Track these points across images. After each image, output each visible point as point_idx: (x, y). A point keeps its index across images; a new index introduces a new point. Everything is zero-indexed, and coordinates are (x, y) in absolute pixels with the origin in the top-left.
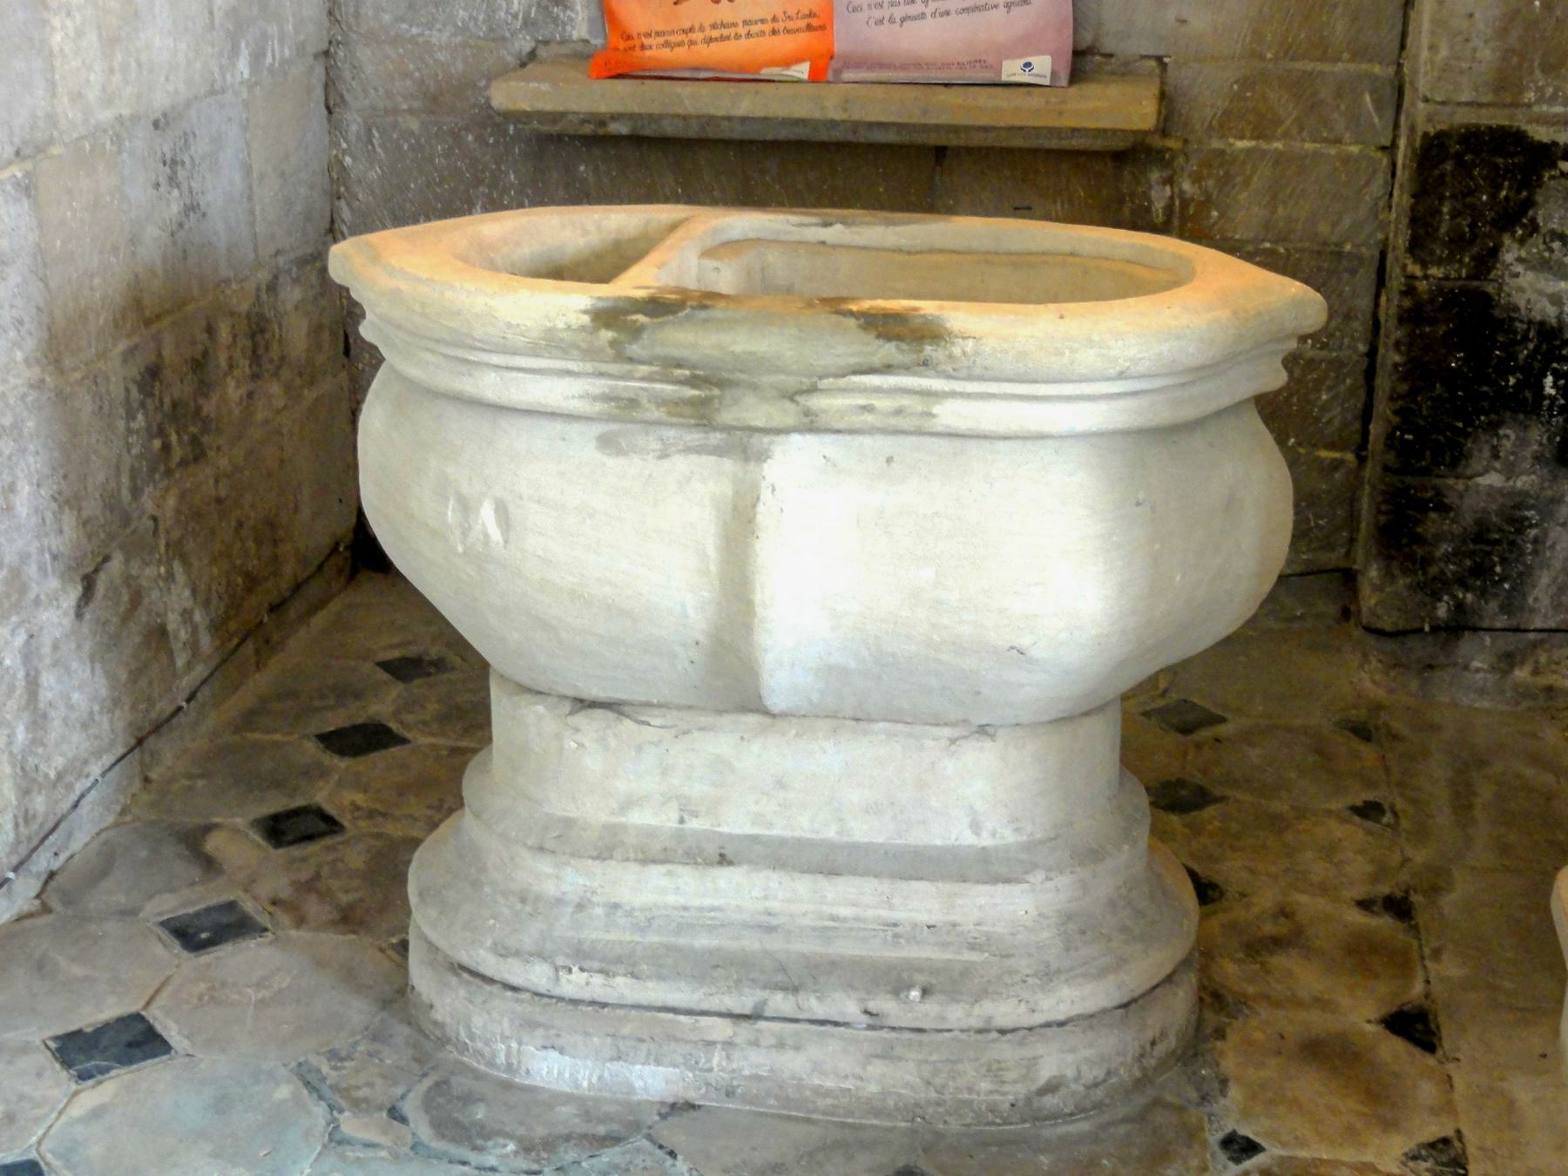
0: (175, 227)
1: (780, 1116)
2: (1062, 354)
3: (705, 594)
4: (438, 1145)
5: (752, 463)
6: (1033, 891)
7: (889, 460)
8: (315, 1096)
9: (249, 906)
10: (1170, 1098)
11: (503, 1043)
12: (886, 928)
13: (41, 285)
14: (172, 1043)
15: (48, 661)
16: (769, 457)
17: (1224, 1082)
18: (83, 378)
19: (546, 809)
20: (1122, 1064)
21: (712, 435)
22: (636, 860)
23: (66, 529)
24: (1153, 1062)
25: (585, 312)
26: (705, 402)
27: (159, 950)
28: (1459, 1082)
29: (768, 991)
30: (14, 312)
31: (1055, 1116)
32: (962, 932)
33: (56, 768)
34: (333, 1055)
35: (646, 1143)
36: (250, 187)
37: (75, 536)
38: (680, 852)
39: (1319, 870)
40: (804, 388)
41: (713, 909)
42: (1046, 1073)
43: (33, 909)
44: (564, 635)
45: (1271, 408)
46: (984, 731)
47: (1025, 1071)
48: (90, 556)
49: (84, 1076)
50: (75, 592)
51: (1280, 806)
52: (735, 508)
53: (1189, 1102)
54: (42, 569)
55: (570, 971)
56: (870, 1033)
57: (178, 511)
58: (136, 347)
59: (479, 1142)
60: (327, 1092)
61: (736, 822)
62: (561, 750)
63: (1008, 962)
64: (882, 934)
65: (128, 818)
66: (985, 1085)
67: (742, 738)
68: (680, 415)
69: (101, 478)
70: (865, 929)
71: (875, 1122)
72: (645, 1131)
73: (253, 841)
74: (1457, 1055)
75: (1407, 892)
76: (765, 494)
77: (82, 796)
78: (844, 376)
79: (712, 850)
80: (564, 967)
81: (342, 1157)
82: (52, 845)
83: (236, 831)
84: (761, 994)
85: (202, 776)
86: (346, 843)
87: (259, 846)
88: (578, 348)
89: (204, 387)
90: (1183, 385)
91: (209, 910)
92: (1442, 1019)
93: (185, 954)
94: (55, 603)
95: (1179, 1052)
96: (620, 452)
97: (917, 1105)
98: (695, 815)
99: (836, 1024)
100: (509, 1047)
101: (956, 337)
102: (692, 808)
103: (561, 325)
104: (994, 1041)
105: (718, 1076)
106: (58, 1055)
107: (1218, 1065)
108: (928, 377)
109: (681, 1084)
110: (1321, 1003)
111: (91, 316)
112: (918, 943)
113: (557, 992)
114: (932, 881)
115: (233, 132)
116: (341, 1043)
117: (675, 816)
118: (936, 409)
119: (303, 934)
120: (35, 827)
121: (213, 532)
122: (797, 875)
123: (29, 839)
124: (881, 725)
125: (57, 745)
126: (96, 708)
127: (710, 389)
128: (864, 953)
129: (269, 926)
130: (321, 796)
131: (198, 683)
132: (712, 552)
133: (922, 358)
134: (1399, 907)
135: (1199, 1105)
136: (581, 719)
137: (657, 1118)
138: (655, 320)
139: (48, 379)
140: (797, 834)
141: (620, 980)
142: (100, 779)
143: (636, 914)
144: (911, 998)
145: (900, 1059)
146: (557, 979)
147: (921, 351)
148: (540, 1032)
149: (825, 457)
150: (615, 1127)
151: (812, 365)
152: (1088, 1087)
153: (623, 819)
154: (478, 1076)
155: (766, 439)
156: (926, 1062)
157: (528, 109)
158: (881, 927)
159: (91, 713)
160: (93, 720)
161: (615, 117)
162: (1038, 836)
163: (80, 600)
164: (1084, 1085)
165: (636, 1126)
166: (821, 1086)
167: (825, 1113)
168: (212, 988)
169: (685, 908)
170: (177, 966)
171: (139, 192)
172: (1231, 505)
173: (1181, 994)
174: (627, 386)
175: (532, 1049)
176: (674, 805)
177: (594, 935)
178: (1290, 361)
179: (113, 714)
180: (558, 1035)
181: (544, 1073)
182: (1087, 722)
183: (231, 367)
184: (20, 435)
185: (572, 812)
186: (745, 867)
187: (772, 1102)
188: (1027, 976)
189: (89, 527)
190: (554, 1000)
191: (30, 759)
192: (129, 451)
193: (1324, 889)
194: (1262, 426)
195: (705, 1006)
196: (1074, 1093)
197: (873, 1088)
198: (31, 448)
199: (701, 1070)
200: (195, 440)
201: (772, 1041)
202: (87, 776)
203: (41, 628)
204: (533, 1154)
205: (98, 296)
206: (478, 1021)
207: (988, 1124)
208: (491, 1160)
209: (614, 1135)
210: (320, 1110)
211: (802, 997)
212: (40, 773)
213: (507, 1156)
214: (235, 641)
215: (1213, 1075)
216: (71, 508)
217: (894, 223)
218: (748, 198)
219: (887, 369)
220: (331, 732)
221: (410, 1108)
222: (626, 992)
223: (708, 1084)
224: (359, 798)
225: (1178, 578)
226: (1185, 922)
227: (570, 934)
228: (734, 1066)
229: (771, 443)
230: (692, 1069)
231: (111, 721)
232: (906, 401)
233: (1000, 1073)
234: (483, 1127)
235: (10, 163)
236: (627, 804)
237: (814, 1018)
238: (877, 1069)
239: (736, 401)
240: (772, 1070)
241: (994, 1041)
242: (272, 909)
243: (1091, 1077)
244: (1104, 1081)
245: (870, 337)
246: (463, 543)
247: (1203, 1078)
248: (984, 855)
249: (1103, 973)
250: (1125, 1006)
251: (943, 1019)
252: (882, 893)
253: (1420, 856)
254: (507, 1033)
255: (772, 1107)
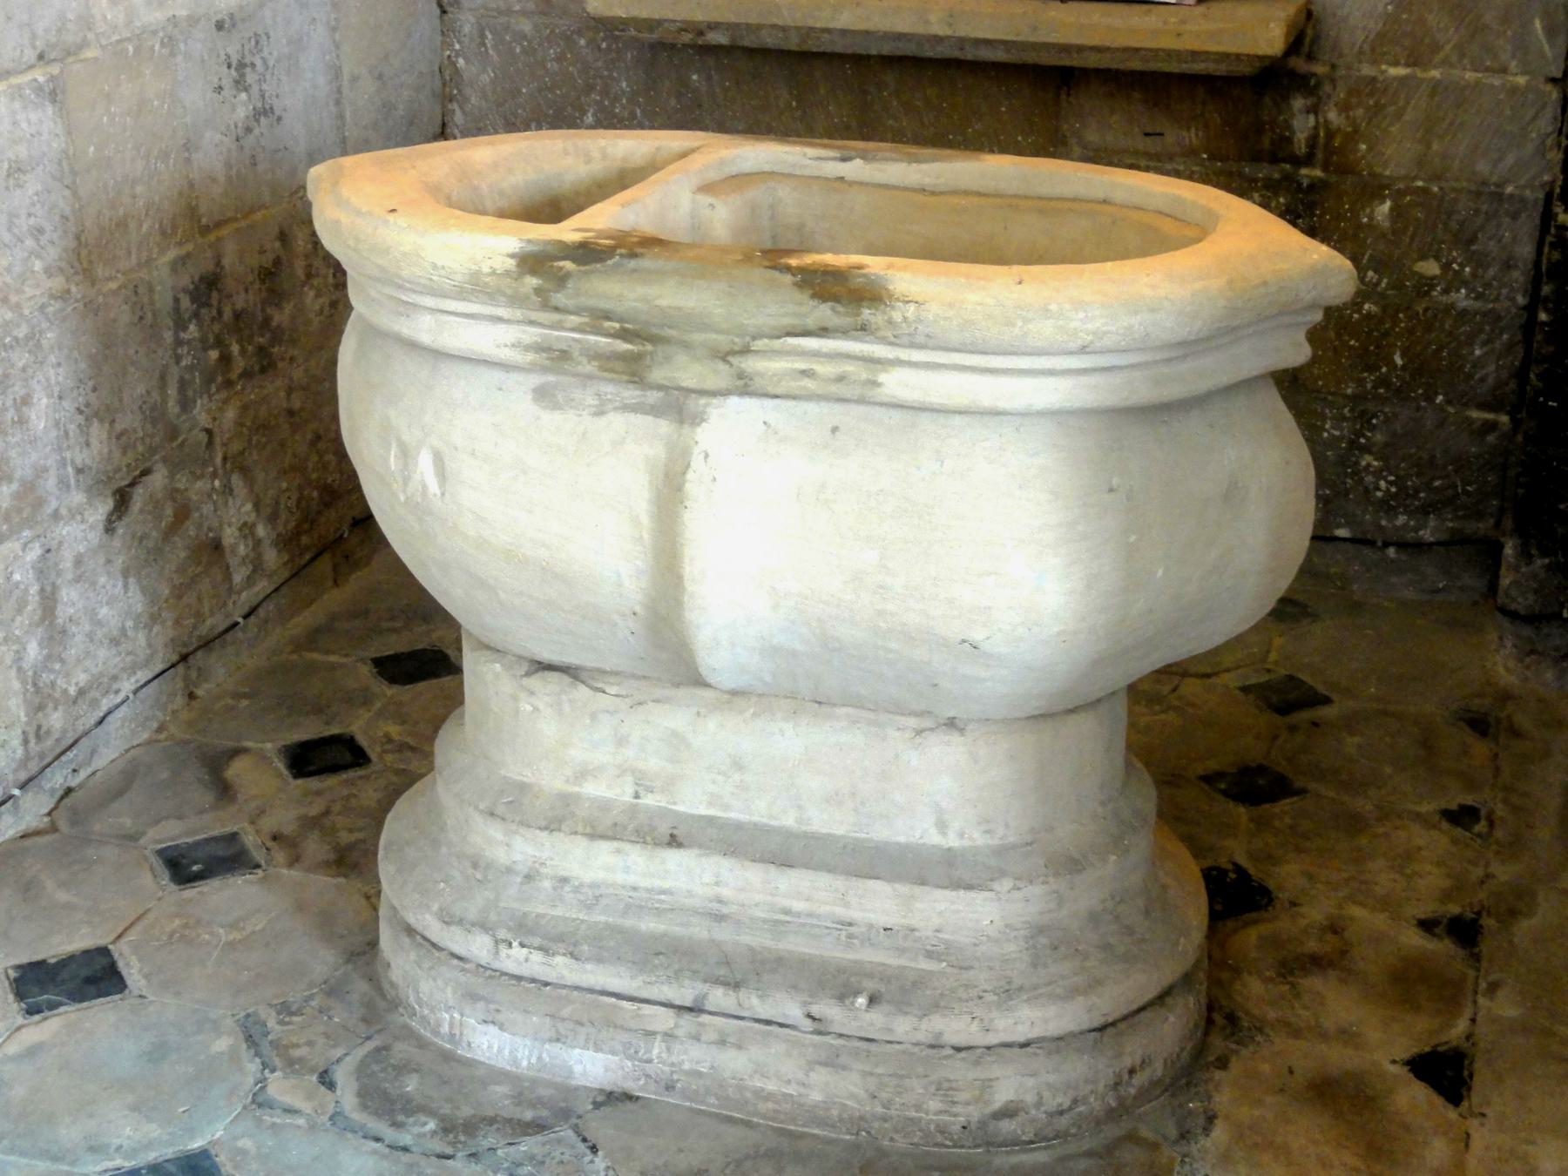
0: (240, 132)
1: (717, 1116)
2: (1013, 325)
3: (638, 562)
4: (358, 1117)
5: (686, 426)
6: (999, 899)
7: (835, 430)
8: (252, 1051)
9: (250, 840)
10: (1145, 1132)
11: (446, 1012)
12: (839, 927)
13: (67, 192)
14: (129, 982)
15: (70, 576)
16: (703, 420)
17: (1211, 1119)
18: (120, 288)
19: (503, 772)
20: (1092, 1092)
21: (649, 393)
22: (584, 834)
23: (94, 442)
24: (1133, 1091)
25: (512, 256)
26: (635, 358)
27: (147, 879)
28: (1477, 1143)
29: (708, 984)
30: (32, 221)
31: (1014, 1143)
32: (920, 938)
33: (77, 684)
34: (285, 1010)
35: (570, 1133)
36: (339, 91)
37: (106, 450)
38: (631, 827)
39: (1384, 879)
40: (737, 348)
41: (664, 892)
42: (1003, 1094)
43: (41, 826)
44: (502, 596)
45: (1290, 383)
46: (951, 724)
47: (977, 1092)
48: (124, 469)
49: (32, 1011)
50: (104, 507)
51: (1364, 805)
52: (667, 475)
53: (1165, 1138)
54: (63, 484)
55: (510, 945)
56: (817, 1038)
57: (239, 424)
58: (188, 255)
59: (401, 1118)
60: (266, 1048)
61: (692, 801)
62: (517, 711)
63: (966, 975)
64: (836, 933)
65: (162, 736)
66: (934, 1105)
67: (698, 713)
68: (612, 371)
69: (141, 389)
70: (818, 926)
71: (816, 1131)
72: (574, 1120)
73: (276, 769)
74: (1484, 1110)
75: (1479, 913)
76: (697, 461)
77: (109, 713)
78: (779, 337)
79: (664, 829)
80: (504, 941)
81: (259, 1121)
82: (72, 761)
83: (262, 757)
84: (701, 987)
85: (245, 696)
86: (367, 778)
87: (281, 775)
88: (504, 294)
89: (275, 296)
90: (1169, 360)
91: (207, 840)
92: (1477, 1065)
93: (173, 887)
94: (79, 518)
95: (1168, 1080)
96: (556, 406)
97: (862, 1118)
98: (651, 790)
99: (781, 1025)
100: (452, 1017)
101: (898, 300)
102: (649, 783)
103: (486, 270)
104: (946, 1057)
105: (659, 1068)
106: (14, 985)
107: (1210, 1098)
108: (867, 342)
109: (620, 1072)
110: (1347, 1036)
111: (132, 225)
112: (872, 945)
113: (496, 965)
114: (889, 881)
115: (319, 35)
116: (294, 997)
117: (630, 790)
118: (882, 378)
119: (295, 874)
120: (49, 742)
121: (282, 445)
122: (748, 863)
123: (42, 756)
124: (844, 710)
125: (79, 661)
126: (130, 624)
127: (644, 345)
128: (812, 951)
129: (263, 863)
130: (358, 726)
131: (261, 597)
132: (645, 520)
133: (859, 323)
134: (1464, 931)
135: (1176, 1142)
136: (535, 682)
137: (591, 1107)
138: (582, 268)
139: (74, 289)
140: (756, 818)
141: (559, 960)
142: (131, 696)
143: (585, 890)
144: (857, 1005)
145: (844, 1068)
146: (497, 953)
147: (858, 315)
148: (481, 1005)
149: (765, 423)
150: (545, 1113)
151: (743, 324)
152: (1051, 1115)
153: (576, 789)
154: (422, 1044)
155: (703, 401)
156: (871, 1074)
157: (624, 16)
158: (834, 925)
159: (123, 631)
160: (126, 636)
161: (714, 26)
162: (1012, 839)
163: (111, 514)
164: (1046, 1112)
165: (565, 1114)
166: (763, 1090)
167: (764, 1117)
168: (186, 926)
169: (635, 889)
170: (160, 899)
171: (196, 96)
172: (1232, 494)
173: (1172, 1019)
174: (562, 336)
175: (473, 1021)
176: (629, 779)
177: (540, 909)
178: (1314, 336)
179: (151, 630)
180: (498, 1011)
181: (485, 1047)
182: (1072, 720)
183: (309, 276)
184: (38, 346)
185: (528, 776)
186: (695, 851)
187: (712, 1100)
188: (985, 991)
189: (124, 438)
190: (498, 974)
191: (44, 675)
192: (177, 363)
193: (1386, 904)
194: (1281, 406)
195: (644, 994)
196: (1033, 1120)
197: (816, 1096)
198: (53, 359)
199: (640, 1060)
200: (261, 351)
201: (713, 1036)
202: (117, 692)
203: (61, 543)
204: (451, 1136)
205: (141, 203)
206: (425, 986)
207: (936, 1145)
208: (406, 1139)
209: (539, 1122)
210: (253, 1067)
211: (743, 993)
212: (59, 690)
213: (423, 1135)
214: (307, 557)
215: (1201, 1110)
216: (101, 421)
217: (918, 161)
218: (757, 126)
219: (823, 332)
220: (388, 657)
221: (341, 1075)
222: (565, 973)
223: (648, 1076)
224: (394, 730)
225: (1160, 573)
226: (1182, 940)
227: (515, 905)
228: (674, 1059)
229: (707, 405)
230: (630, 1058)
231: (148, 639)
232: (849, 368)
233: (950, 1093)
234: (409, 1101)
235: (31, 67)
236: (582, 774)
237: (756, 1017)
238: (820, 1076)
239: (668, 359)
240: (712, 1067)
241: (946, 1057)
242: (270, 844)
243: (1055, 1104)
244: (1070, 1109)
245: (803, 296)
246: (404, 491)
247: (1190, 1112)
248: (949, 858)
249: (1073, 993)
250: (1102, 1029)
251: (890, 1030)
252: (837, 890)
253: (1504, 872)
254: (451, 1003)
255: (713, 1105)
